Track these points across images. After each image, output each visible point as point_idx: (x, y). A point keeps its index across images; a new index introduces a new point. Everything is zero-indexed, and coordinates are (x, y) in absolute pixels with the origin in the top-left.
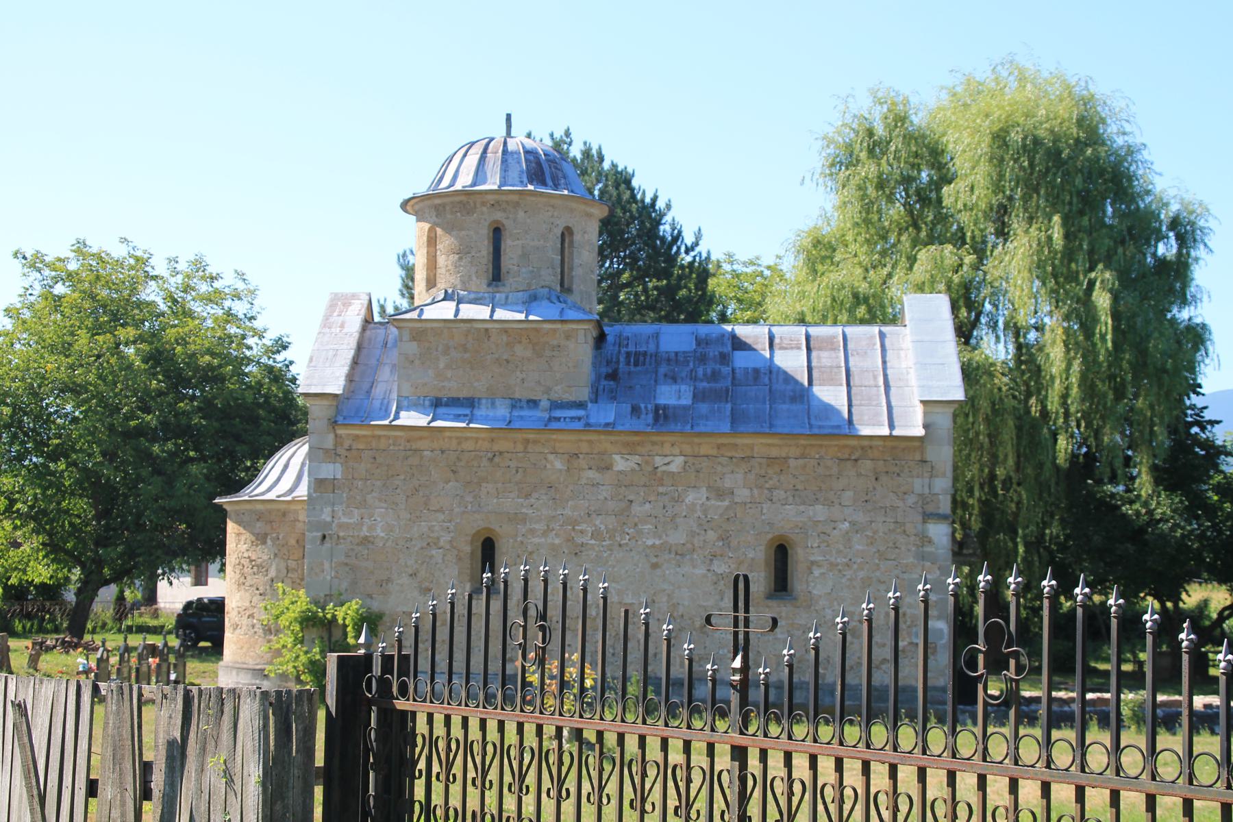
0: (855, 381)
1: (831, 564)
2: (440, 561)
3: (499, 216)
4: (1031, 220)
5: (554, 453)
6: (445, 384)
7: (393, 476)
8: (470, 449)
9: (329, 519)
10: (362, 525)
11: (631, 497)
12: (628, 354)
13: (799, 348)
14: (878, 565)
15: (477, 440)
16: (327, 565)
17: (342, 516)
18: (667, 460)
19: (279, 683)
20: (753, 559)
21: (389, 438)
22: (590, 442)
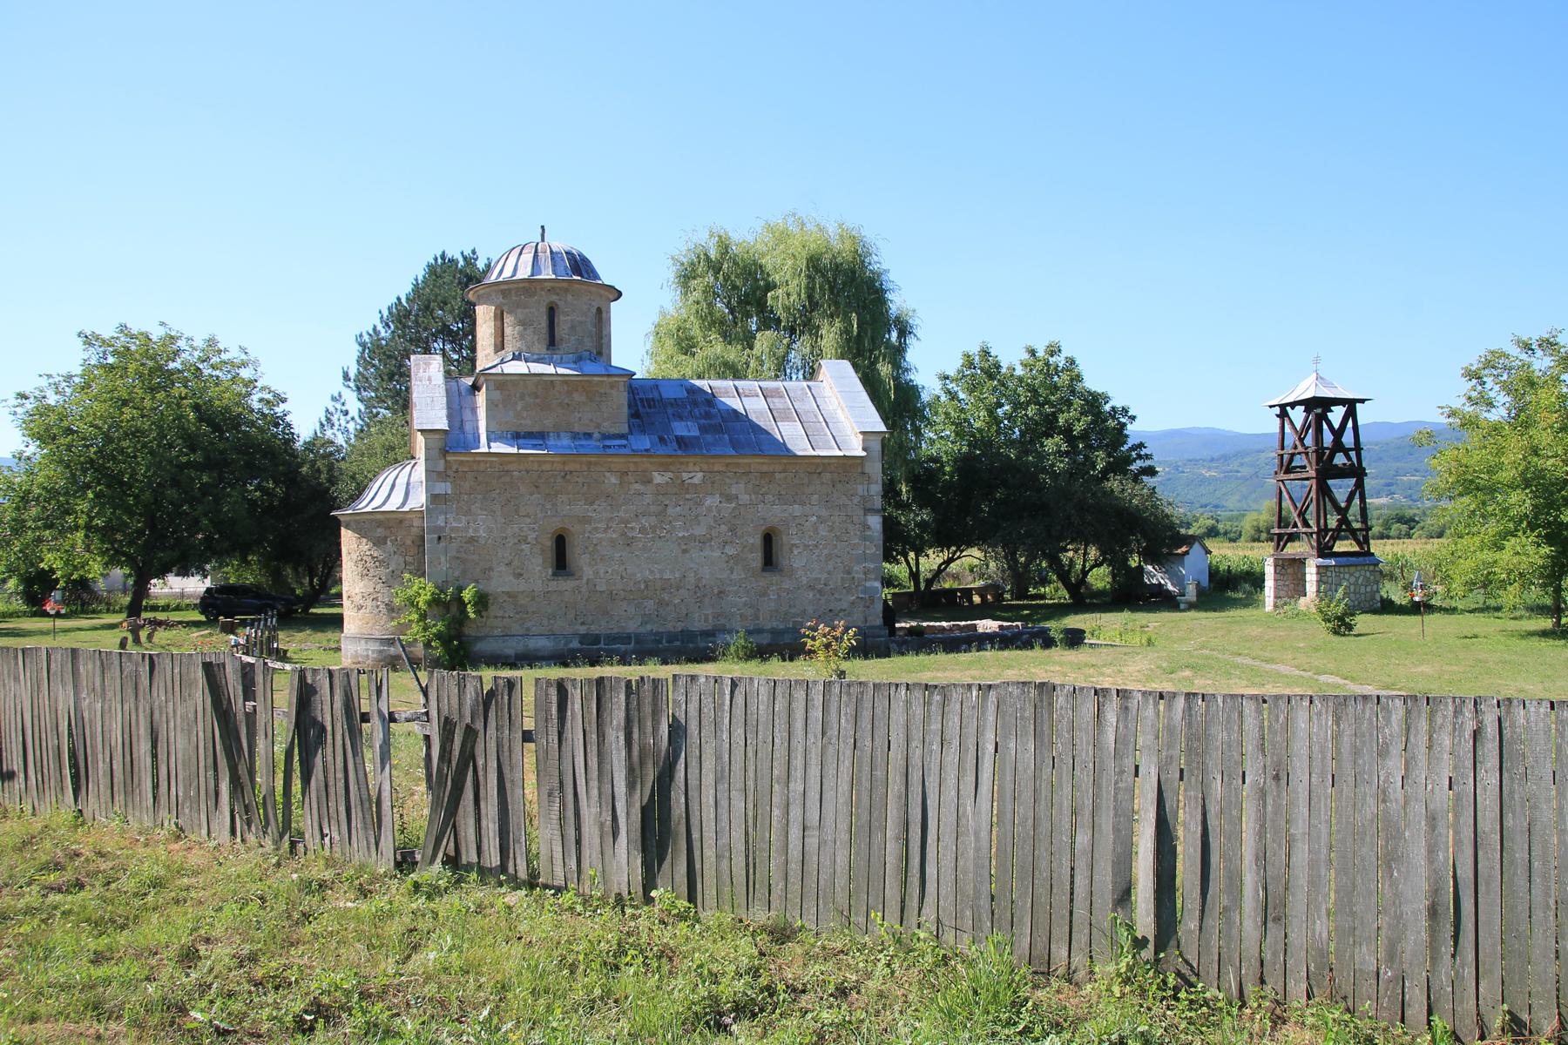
0: (804, 418)
1: (805, 545)
3: (554, 298)
4: (832, 316)
5: (610, 471)
11: (667, 502)
12: (641, 400)
13: (734, 397)
15: (553, 462)
16: (443, 559)
17: (453, 522)
18: (693, 474)
20: (753, 544)
21: (486, 462)
22: (635, 463)
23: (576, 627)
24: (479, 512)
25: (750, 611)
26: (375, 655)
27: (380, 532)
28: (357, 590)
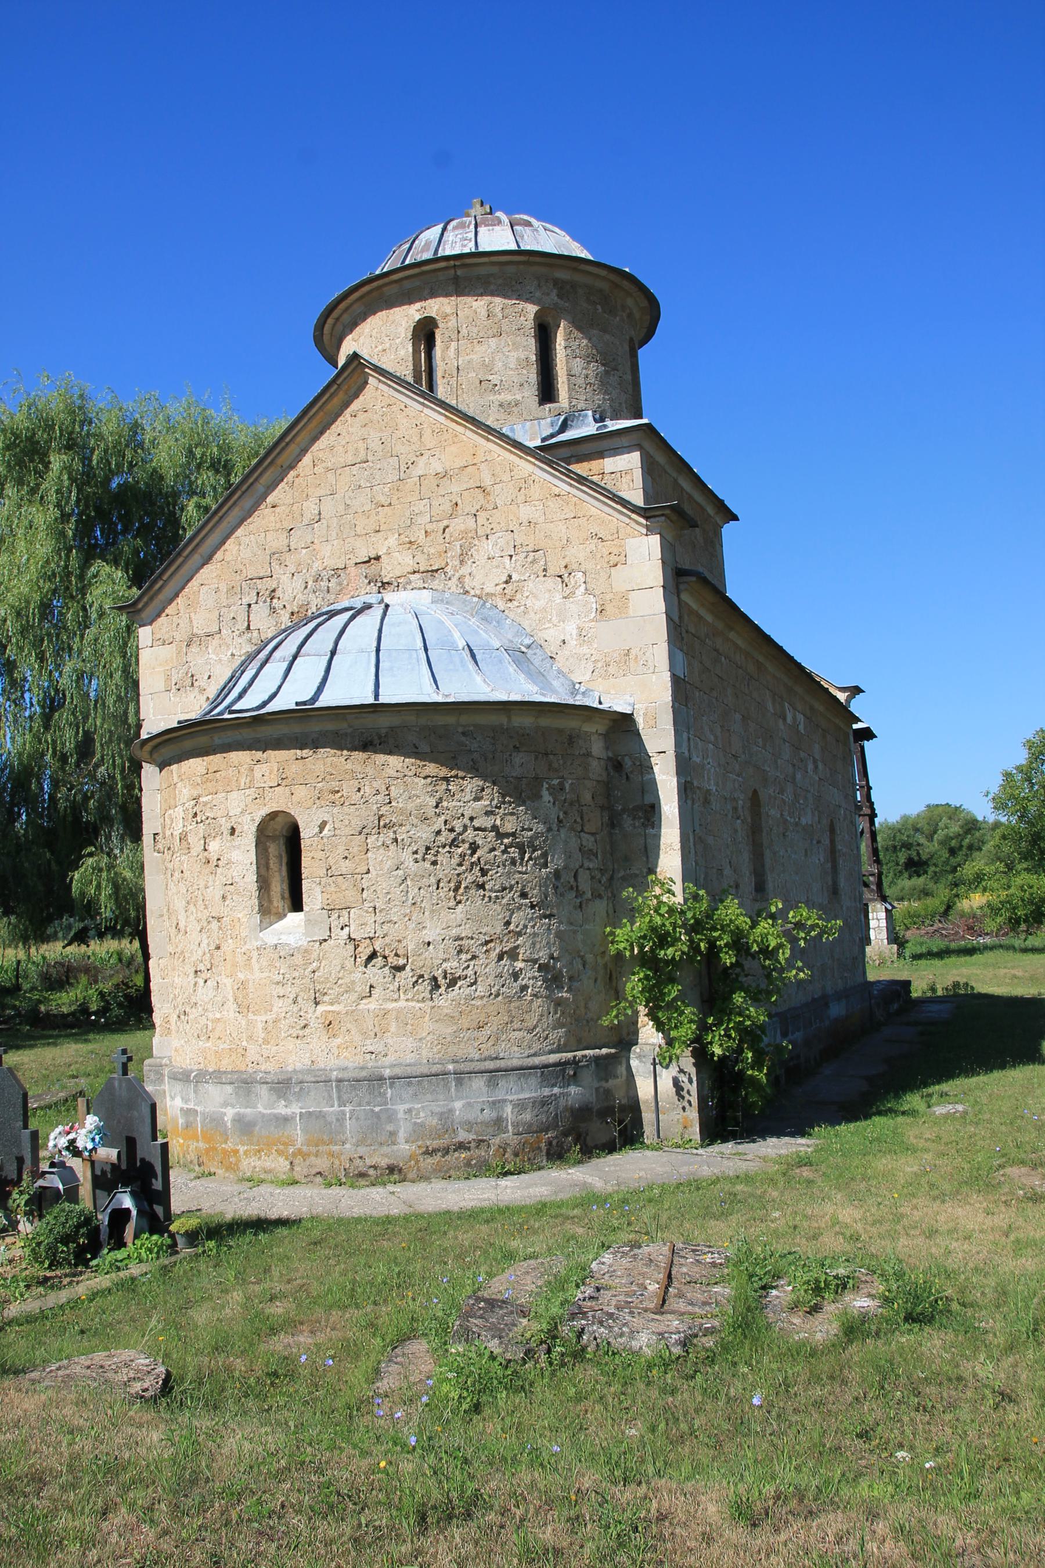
19: (596, 1084)
26: (527, 1116)
27: (521, 763)
28: (429, 935)
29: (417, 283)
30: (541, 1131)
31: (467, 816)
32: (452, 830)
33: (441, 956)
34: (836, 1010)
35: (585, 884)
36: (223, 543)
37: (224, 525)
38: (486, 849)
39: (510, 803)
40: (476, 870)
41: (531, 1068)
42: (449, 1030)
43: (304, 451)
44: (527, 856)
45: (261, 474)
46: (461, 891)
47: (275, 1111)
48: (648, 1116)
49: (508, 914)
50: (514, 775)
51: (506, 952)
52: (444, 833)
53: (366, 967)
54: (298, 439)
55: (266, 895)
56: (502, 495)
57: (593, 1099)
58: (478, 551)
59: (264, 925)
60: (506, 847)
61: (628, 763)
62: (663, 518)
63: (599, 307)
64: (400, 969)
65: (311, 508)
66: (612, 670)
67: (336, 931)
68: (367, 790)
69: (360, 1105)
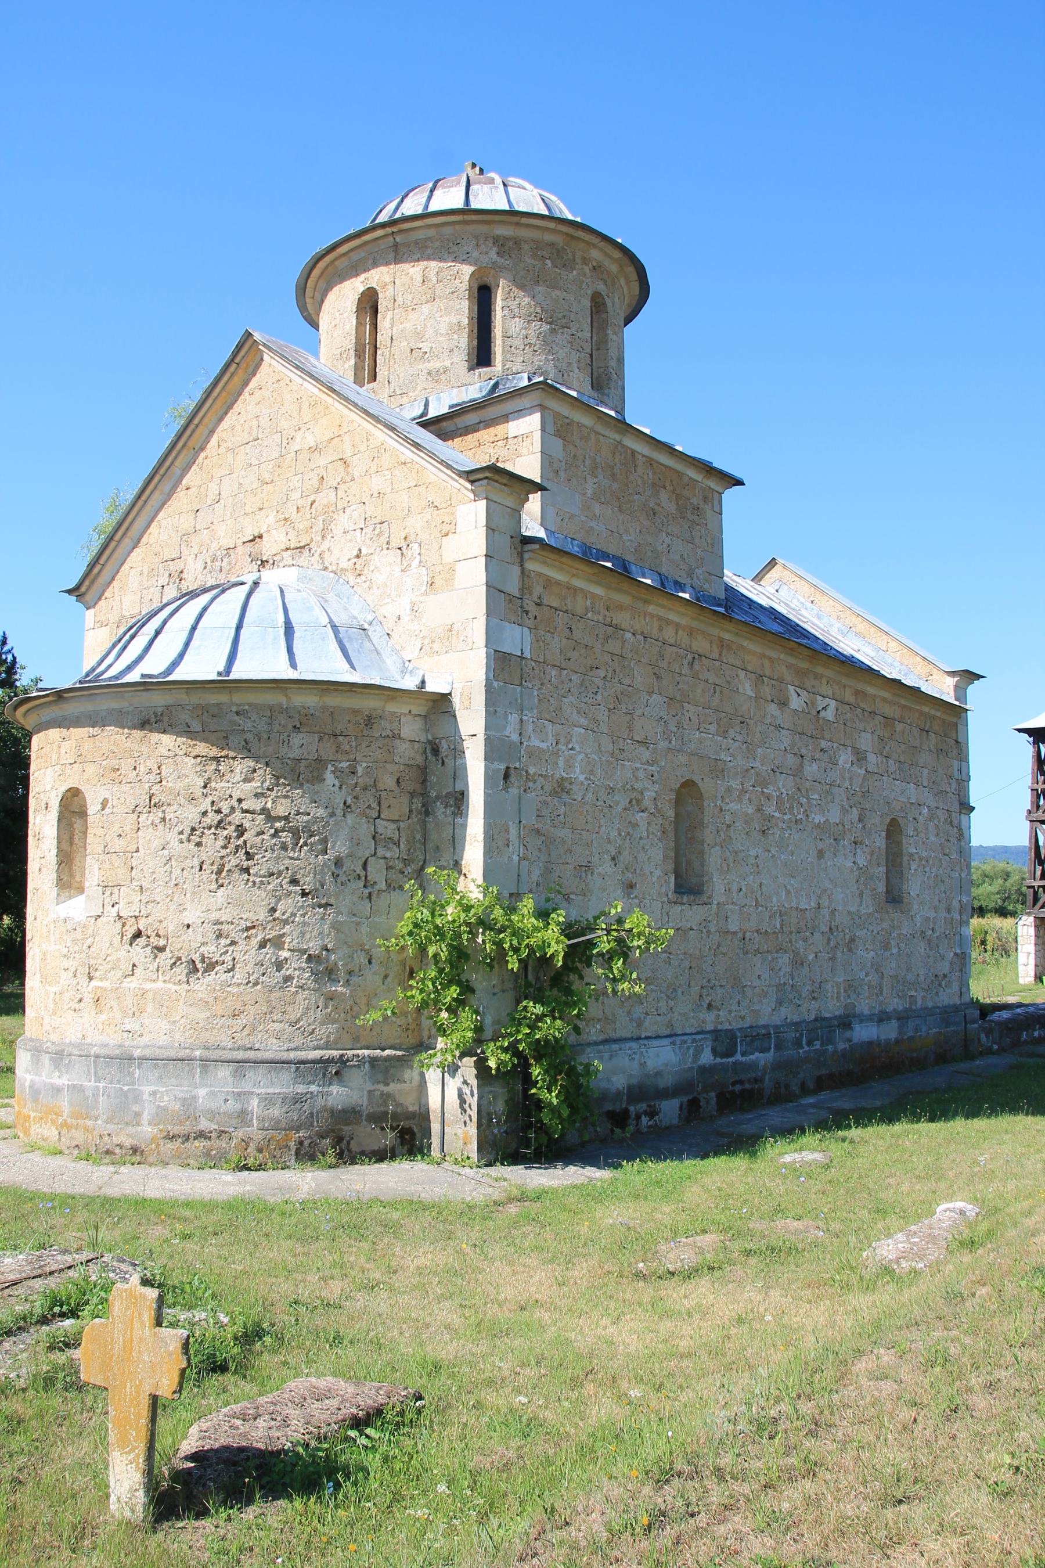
2: (645, 834)
3: (601, 287)
6: (592, 524)
7: (591, 668)
8: (672, 641)
9: (515, 737)
10: (556, 753)
11: (803, 752)
14: (941, 860)
15: (677, 625)
19: (369, 1086)
22: (770, 658)
23: (702, 1016)
24: (575, 717)
25: (873, 978)
26: (276, 1112)
27: (301, 746)
28: (192, 915)
29: (362, 254)
30: (291, 1129)
31: (235, 798)
32: (219, 812)
33: (200, 939)
34: (863, 1033)
35: (377, 872)
36: (148, 526)
37: (148, 509)
38: (253, 832)
39: (284, 784)
40: (241, 853)
41: (283, 1062)
42: (203, 1016)
43: (212, 432)
44: (302, 841)
45: (176, 458)
46: (224, 874)
47: (52, 1081)
48: (435, 1127)
49: (273, 900)
50: (292, 756)
51: (269, 940)
52: (211, 814)
53: (131, 945)
54: (206, 420)
55: (66, 870)
56: (358, 466)
57: (365, 1102)
58: (336, 525)
59: (62, 898)
60: (277, 831)
61: (444, 746)
62: (486, 481)
63: (548, 262)
64: (161, 949)
65: (213, 488)
66: (436, 646)
67: (108, 907)
68: (142, 769)
69: (111, 1083)
